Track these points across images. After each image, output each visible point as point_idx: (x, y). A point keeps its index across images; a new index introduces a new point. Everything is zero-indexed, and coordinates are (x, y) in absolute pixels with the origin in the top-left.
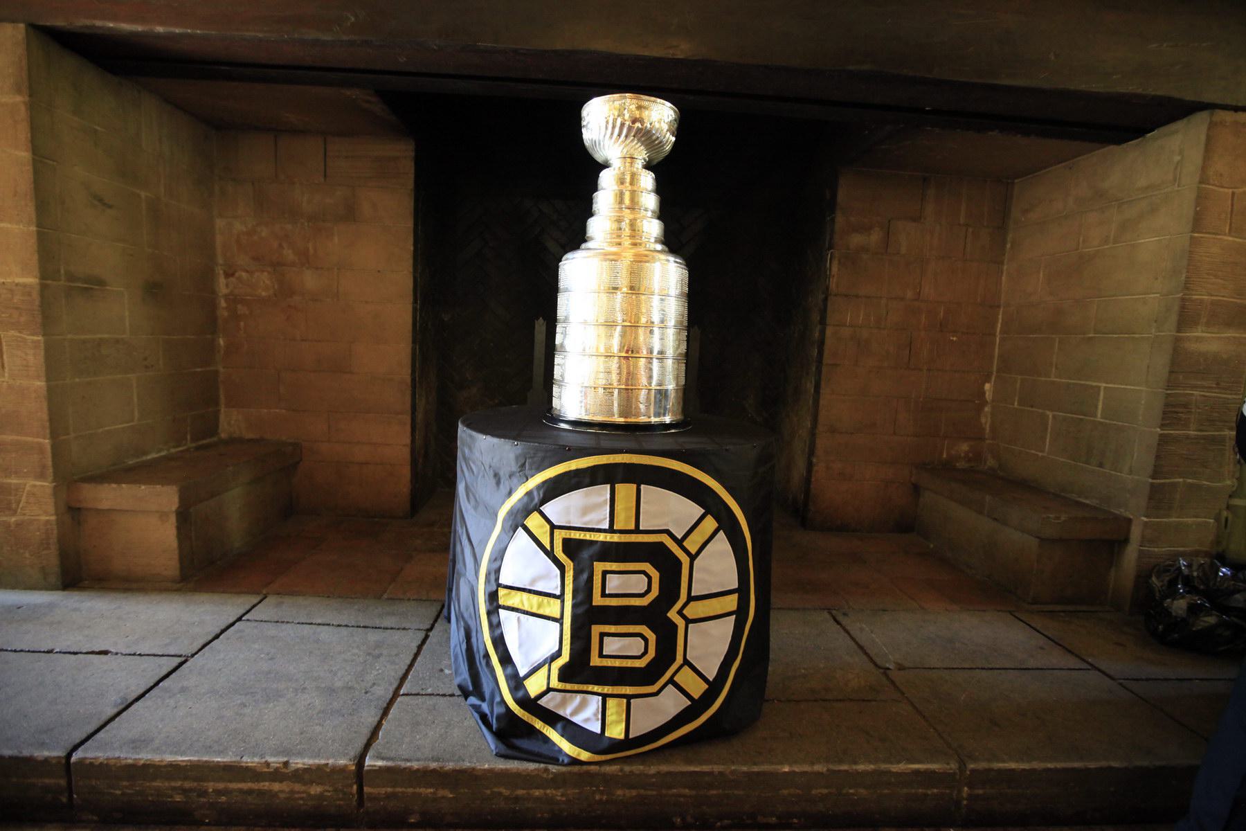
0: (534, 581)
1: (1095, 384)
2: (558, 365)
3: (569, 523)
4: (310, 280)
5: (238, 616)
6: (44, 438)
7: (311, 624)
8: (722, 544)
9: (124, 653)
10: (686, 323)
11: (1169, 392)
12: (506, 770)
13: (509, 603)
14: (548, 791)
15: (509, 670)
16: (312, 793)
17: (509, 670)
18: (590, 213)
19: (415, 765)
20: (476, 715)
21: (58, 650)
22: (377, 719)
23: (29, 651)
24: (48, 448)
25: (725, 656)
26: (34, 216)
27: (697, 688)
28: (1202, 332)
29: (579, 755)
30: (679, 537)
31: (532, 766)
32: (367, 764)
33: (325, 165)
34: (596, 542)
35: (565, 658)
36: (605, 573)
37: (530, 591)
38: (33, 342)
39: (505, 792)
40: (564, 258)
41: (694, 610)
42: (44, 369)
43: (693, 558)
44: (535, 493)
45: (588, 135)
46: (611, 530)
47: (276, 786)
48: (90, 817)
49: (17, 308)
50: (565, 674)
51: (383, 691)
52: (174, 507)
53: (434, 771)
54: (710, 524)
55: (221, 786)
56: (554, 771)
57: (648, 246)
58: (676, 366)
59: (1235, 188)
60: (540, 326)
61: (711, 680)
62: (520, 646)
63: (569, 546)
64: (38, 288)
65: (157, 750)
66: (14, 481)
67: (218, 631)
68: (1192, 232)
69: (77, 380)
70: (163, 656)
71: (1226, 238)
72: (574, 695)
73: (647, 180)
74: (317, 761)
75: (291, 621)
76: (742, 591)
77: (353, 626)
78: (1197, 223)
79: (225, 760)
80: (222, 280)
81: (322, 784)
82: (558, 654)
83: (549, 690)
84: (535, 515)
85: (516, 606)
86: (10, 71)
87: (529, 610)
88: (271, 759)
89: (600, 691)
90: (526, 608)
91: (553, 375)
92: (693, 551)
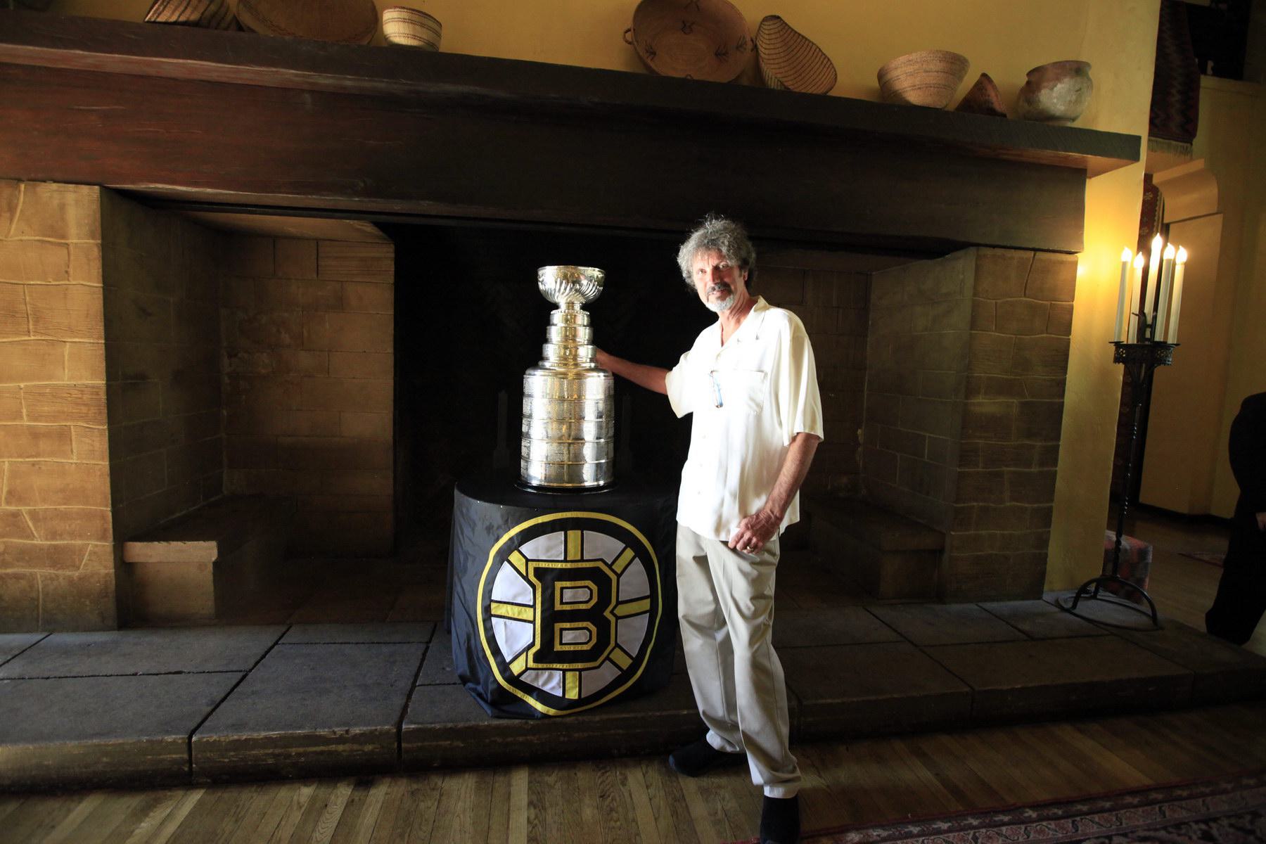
0: (515, 597)
1: (922, 433)
2: (525, 446)
3: (538, 557)
4: (305, 360)
5: (274, 641)
6: (107, 506)
7: (335, 643)
8: (638, 566)
9: (195, 672)
10: (613, 415)
11: (963, 441)
12: (500, 724)
13: (498, 613)
14: (528, 738)
15: (499, 659)
16: (366, 750)
17: (499, 659)
18: (546, 341)
19: (438, 726)
20: (473, 694)
21: (141, 673)
22: (404, 701)
23: (117, 675)
24: (110, 514)
25: (643, 641)
26: (103, 333)
27: (625, 663)
28: (982, 399)
29: (548, 711)
30: (610, 563)
31: (517, 721)
32: (404, 727)
33: (317, 263)
34: (556, 569)
35: (538, 646)
36: (562, 589)
37: (512, 604)
38: (98, 429)
39: (499, 740)
40: (528, 372)
41: (621, 610)
42: (108, 451)
43: (619, 576)
44: (515, 538)
45: (541, 287)
46: (565, 561)
47: (341, 748)
48: (205, 780)
49: (87, 404)
50: (538, 658)
51: (405, 684)
52: (214, 559)
53: (451, 728)
54: (629, 553)
55: (301, 750)
56: (532, 723)
57: (584, 365)
58: (606, 446)
59: (999, 299)
60: (503, 396)
61: (634, 656)
62: (507, 641)
63: (539, 573)
64: (104, 389)
65: (253, 729)
66: (79, 542)
67: (262, 652)
68: (971, 329)
69: (128, 458)
70: (227, 672)
71: (993, 333)
72: (544, 671)
73: (582, 318)
74: (369, 728)
75: (318, 641)
76: (653, 596)
77: (368, 643)
78: (973, 324)
79: (304, 732)
80: (226, 361)
81: (374, 743)
82: (533, 644)
83: (527, 669)
84: (516, 553)
85: (503, 614)
86: (86, 221)
87: (512, 616)
88: (336, 730)
89: (561, 667)
90: (510, 615)
91: (521, 453)
92: (619, 572)
